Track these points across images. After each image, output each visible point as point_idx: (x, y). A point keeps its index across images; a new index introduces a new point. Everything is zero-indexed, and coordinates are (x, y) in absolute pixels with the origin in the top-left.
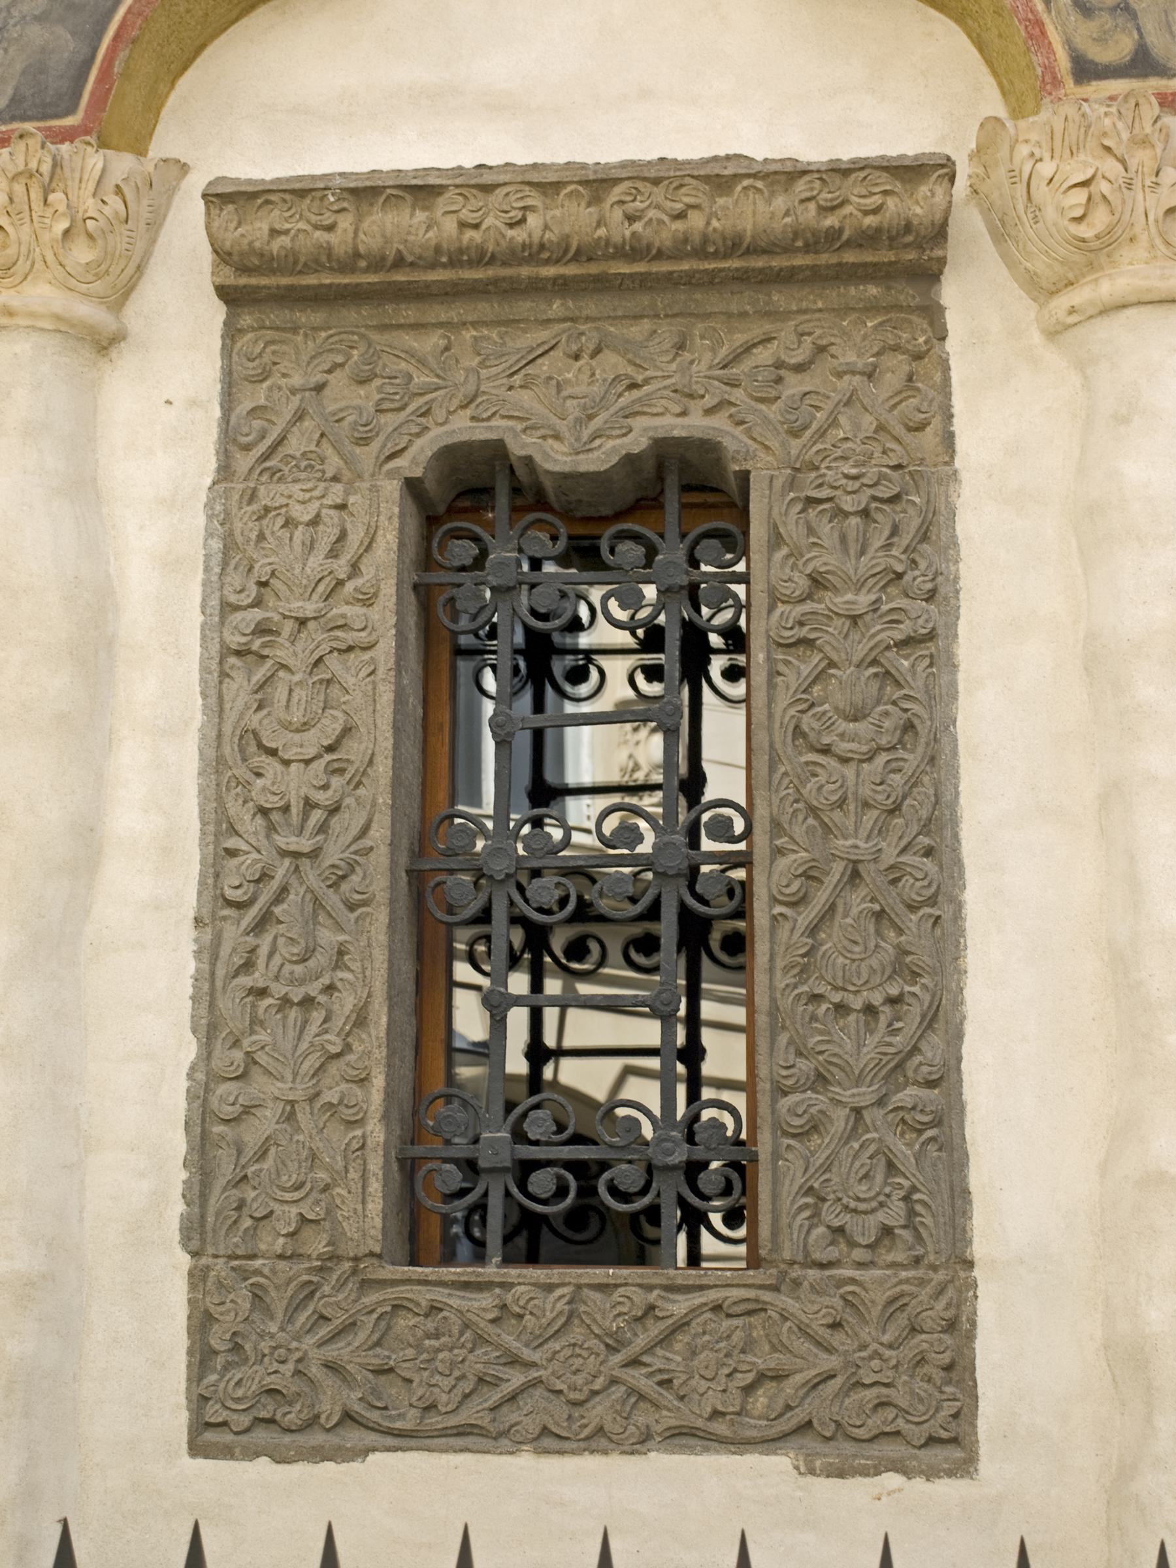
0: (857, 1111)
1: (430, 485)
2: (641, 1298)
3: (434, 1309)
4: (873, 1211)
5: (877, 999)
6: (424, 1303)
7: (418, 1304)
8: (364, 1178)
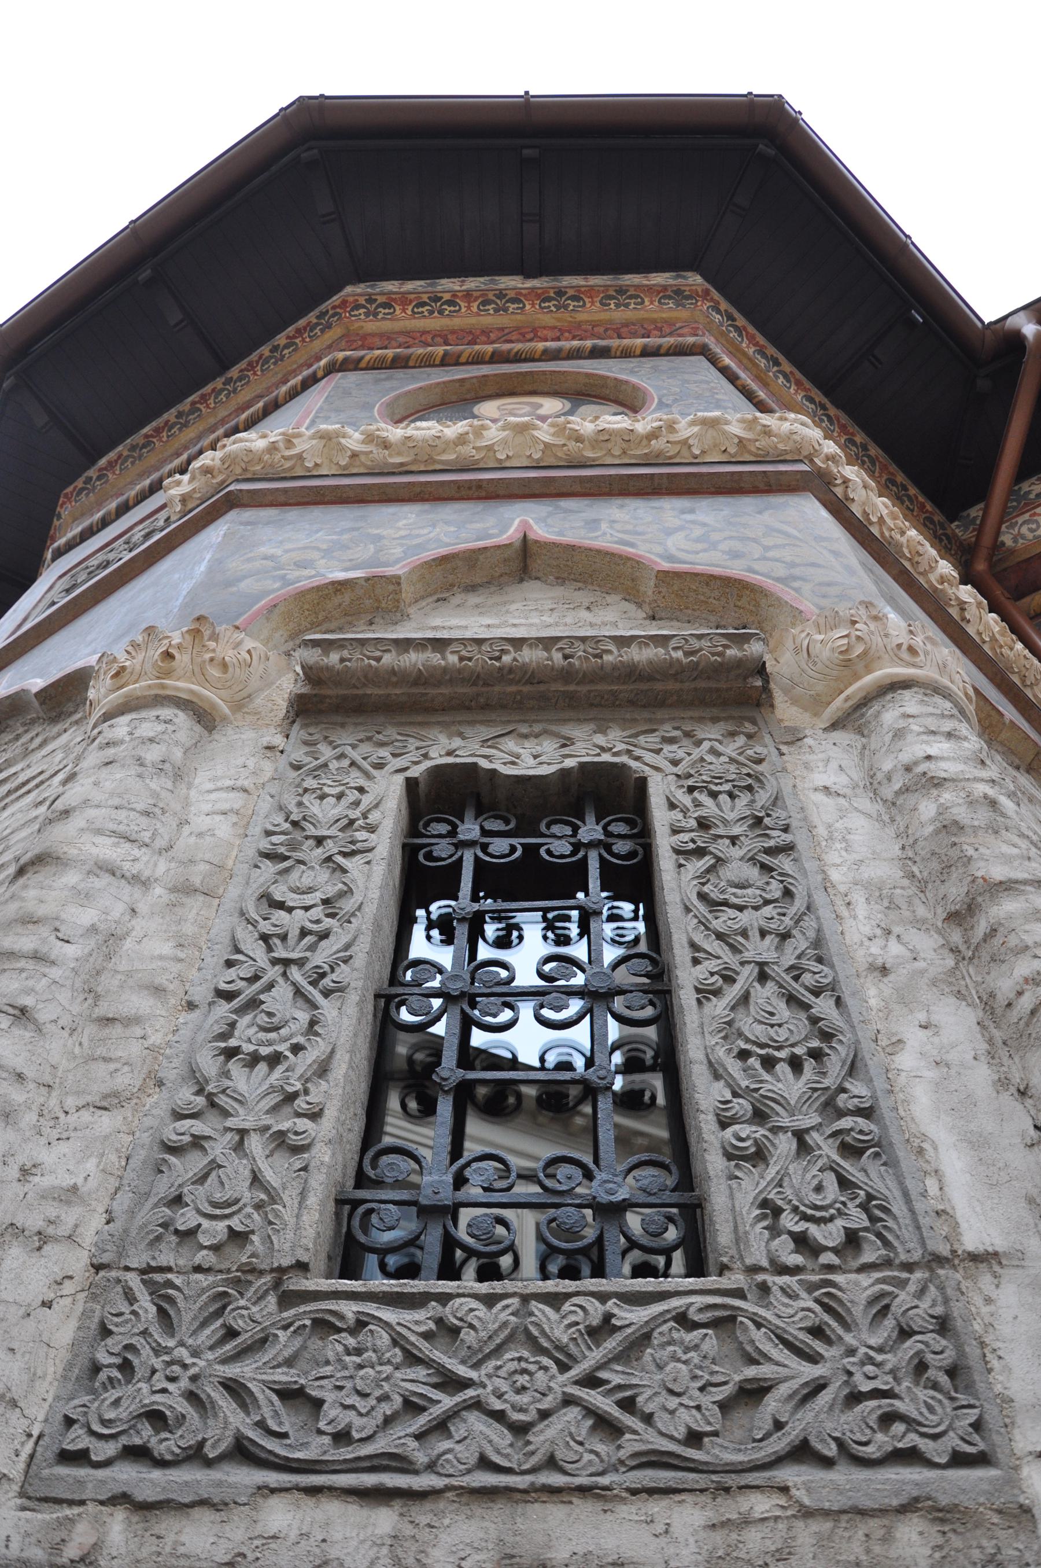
0: (800, 1135)
1: (422, 787)
2: (596, 1310)
3: (361, 1324)
4: (831, 1219)
5: (799, 1051)
6: (350, 1315)
7: (341, 1317)
8: (303, 1195)
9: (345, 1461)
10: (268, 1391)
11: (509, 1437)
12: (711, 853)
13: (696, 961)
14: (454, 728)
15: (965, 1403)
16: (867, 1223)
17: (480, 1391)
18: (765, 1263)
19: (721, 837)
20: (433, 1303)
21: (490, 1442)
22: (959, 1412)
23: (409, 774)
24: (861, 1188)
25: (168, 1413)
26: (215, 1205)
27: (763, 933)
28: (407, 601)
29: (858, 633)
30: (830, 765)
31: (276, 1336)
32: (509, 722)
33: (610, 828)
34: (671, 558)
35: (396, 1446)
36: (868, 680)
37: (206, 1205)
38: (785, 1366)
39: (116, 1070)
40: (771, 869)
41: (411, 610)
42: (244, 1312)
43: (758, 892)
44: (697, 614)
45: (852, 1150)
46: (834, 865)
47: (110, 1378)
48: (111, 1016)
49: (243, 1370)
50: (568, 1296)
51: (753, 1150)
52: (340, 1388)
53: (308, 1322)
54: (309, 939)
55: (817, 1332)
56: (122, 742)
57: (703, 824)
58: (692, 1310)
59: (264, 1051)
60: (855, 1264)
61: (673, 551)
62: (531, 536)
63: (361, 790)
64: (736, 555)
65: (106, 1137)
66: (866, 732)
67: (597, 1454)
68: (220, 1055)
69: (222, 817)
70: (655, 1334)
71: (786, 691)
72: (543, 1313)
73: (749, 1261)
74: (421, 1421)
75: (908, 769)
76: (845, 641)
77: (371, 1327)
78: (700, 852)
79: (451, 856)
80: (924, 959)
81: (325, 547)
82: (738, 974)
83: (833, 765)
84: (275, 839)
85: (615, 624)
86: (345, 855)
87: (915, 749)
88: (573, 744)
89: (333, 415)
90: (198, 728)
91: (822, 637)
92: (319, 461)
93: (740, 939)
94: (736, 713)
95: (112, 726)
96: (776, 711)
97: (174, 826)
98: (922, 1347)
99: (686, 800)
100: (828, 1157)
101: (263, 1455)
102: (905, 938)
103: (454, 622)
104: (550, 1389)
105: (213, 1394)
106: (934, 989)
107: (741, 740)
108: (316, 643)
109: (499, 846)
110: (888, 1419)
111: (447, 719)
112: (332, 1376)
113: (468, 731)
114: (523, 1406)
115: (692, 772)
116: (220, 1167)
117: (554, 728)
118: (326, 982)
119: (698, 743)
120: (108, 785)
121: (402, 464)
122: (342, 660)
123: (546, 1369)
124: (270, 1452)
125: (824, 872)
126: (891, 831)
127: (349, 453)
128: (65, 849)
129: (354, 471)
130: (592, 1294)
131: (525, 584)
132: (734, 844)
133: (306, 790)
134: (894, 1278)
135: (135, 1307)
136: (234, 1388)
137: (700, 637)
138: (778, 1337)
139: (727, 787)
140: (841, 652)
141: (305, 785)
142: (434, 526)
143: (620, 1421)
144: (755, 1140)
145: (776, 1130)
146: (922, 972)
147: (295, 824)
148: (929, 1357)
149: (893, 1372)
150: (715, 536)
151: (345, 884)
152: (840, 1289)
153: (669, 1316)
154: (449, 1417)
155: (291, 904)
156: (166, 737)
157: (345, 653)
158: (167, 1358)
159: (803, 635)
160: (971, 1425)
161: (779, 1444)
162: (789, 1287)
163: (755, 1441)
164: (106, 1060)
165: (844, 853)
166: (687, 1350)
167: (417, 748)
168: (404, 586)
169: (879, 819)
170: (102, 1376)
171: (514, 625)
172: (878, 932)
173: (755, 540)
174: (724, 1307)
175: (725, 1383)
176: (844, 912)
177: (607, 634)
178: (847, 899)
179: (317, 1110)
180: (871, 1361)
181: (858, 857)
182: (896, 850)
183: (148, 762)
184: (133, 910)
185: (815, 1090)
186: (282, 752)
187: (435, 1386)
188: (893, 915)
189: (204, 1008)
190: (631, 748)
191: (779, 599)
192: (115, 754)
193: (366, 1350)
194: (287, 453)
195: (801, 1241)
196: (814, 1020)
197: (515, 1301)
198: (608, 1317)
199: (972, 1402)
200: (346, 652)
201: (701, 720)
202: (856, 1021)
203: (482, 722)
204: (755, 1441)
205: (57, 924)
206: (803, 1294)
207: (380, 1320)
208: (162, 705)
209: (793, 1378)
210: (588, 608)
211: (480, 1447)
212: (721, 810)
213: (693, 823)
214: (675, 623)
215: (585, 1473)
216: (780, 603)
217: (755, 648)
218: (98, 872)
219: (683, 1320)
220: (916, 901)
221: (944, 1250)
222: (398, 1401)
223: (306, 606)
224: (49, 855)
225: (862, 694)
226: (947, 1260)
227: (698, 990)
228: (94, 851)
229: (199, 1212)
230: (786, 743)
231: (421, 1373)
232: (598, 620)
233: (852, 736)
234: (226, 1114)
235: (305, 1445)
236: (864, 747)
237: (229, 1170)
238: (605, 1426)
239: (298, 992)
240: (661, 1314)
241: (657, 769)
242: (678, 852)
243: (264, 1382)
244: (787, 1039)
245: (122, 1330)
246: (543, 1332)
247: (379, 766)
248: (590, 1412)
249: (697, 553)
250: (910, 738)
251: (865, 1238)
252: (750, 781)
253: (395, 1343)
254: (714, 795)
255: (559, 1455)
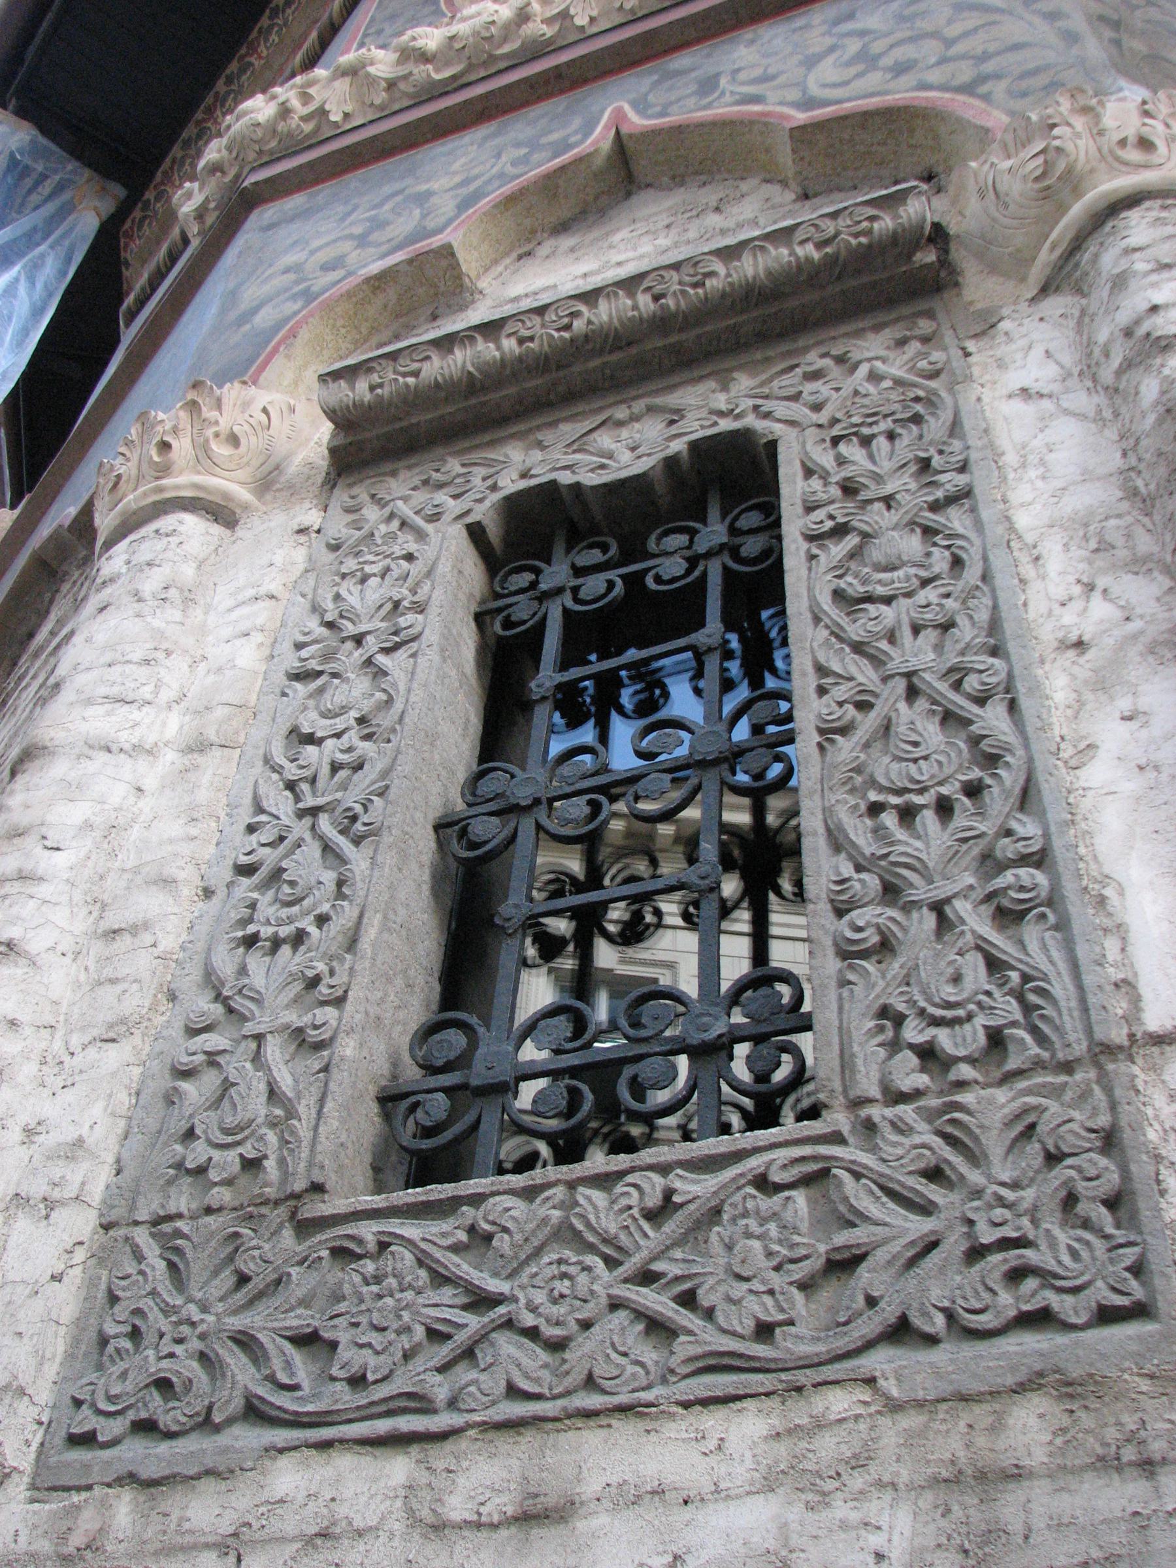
0: (938, 908)
3: (383, 1246)
4: (970, 1017)
7: (360, 1241)
9: (358, 1408)
10: (278, 1339)
11: (543, 1356)
12: (855, 529)
13: (822, 691)
14: (531, 437)
15: (1121, 1241)
16: (1018, 1016)
17: (513, 1307)
18: (875, 1092)
19: (870, 501)
20: (464, 1208)
21: (519, 1365)
22: (1113, 1254)
23: (469, 519)
24: (1014, 968)
25: (174, 1379)
26: (227, 1132)
27: (916, 630)
28: (473, 274)
29: (1057, 143)
30: (1032, 353)
31: (289, 1274)
32: (601, 409)
33: (738, 524)
34: (809, 103)
35: (414, 1384)
36: (1077, 210)
37: (218, 1133)
38: (885, 1224)
39: (125, 991)
40: (936, 532)
41: (482, 284)
42: (256, 1253)
43: (913, 571)
44: (860, 173)
45: (1009, 916)
46: (1022, 505)
47: (118, 1351)
48: (116, 927)
49: (253, 1321)
50: (621, 1174)
51: (876, 939)
52: (356, 1325)
53: (325, 1253)
54: (342, 774)
55: (934, 1174)
56: (119, 575)
57: (849, 489)
58: (774, 1168)
59: (285, 931)
60: (997, 1074)
61: (814, 90)
62: (624, 130)
63: (409, 557)
64: (900, 69)
65: (114, 1074)
66: (1085, 289)
67: (641, 1364)
68: (238, 946)
69: (243, 640)
70: (726, 1208)
71: (980, 255)
72: (589, 1199)
73: (852, 1094)
74: (444, 1351)
75: (1128, 333)
76: (1040, 160)
77: (393, 1248)
78: (840, 531)
79: (535, 614)
80: (1141, 617)
81: (358, 230)
82: (876, 695)
83: (1038, 352)
84: (304, 653)
85: (754, 222)
86: (387, 651)
87: (1133, 303)
88: (683, 417)
89: (386, 26)
90: (217, 529)
91: (1008, 164)
92: (348, 109)
93: (884, 645)
94: (906, 310)
95: (110, 558)
96: (964, 292)
97: (185, 667)
98: (1073, 1173)
99: (826, 459)
100: (973, 932)
101: (274, 1413)
102: (1115, 591)
103: (540, 283)
104: (592, 1292)
105: (220, 1351)
106: (1151, 659)
107: (915, 346)
108: (336, 375)
109: (594, 585)
110: (1016, 1275)
111: (522, 427)
112: (347, 1313)
113: (547, 436)
114: (554, 1317)
115: (839, 415)
116: (234, 1084)
117: (659, 401)
118: (359, 827)
119: (855, 367)
120: (100, 638)
121: (454, 78)
122: (372, 388)
123: (587, 1269)
124: (279, 1408)
125: (1008, 518)
126: (1112, 433)
127: (384, 84)
128: (52, 734)
129: (397, 107)
130: (651, 1168)
131: (634, 199)
132: (889, 507)
133: (344, 576)
134: (1044, 1085)
135: (143, 1267)
136: (245, 1342)
137: (834, 215)
138: (882, 1188)
139: (883, 426)
140: (1037, 179)
141: (344, 570)
142: (498, 156)
143: (673, 1321)
144: (878, 926)
145: (908, 907)
146: (1135, 637)
147: (330, 625)
148: (1081, 1186)
149: (1034, 1214)
150: (877, 47)
151: (384, 691)
152: (969, 1112)
153: (743, 1181)
154: (477, 1342)
155: (319, 734)
156: (169, 554)
157: (375, 378)
158: (174, 1319)
159: (987, 166)
160: (1127, 1269)
161: (869, 1325)
162: (901, 1119)
163: (839, 1324)
164: (113, 981)
165: (1039, 484)
166: (763, 1221)
167: (484, 479)
168: (461, 255)
169: (1099, 419)
170: (110, 1349)
171: (619, 264)
172: (1077, 590)
173: (935, 35)
174: (815, 1158)
175: (806, 1257)
176: (1027, 570)
177: (706, 250)
178: (1035, 552)
179: (340, 993)
180: (1001, 1202)
181: (1059, 484)
182: (1116, 461)
183: (146, 594)
184: (139, 790)
185: (965, 840)
186: (318, 532)
187: (465, 1307)
188: (1101, 561)
189: (221, 893)
190: (759, 402)
191: (959, 120)
192: (111, 595)
193: (386, 1276)
194: (305, 111)
195: (928, 1054)
196: (975, 741)
197: (559, 1192)
198: (668, 1194)
199: (1132, 1238)
200: (375, 376)
201: (858, 333)
202: (1030, 729)
203: (566, 419)
204: (839, 1324)
205: (44, 831)
206: (922, 1126)
207: (402, 1237)
208: (166, 513)
209: (894, 1238)
210: (717, 209)
211: (507, 1373)
212: (874, 462)
213: (835, 492)
214: (837, 196)
215: (625, 1389)
216: (962, 124)
217: (918, 209)
218: (90, 752)
219: (762, 1183)
220: (1139, 531)
221: (1118, 1035)
222: (419, 1332)
223: (340, 323)
224: (35, 747)
225: (1069, 236)
226: (1121, 1048)
227: (821, 731)
228: (84, 727)
229: (210, 1143)
230: (975, 336)
231: (447, 1294)
232: (730, 223)
233: (1069, 298)
234: (244, 1019)
235: (316, 1396)
236: (1083, 312)
237: (242, 1088)
238: (658, 1328)
239: (327, 848)
240: (734, 1180)
241: (792, 423)
242: (811, 538)
243: (274, 1330)
244: (933, 776)
245: (128, 1294)
246: (588, 1224)
247: (434, 518)
248: (639, 1314)
249: (846, 83)
250: (1133, 284)
251: (1012, 1036)
252: (919, 408)
253: (420, 1263)
254: (866, 442)
255: (597, 1372)
